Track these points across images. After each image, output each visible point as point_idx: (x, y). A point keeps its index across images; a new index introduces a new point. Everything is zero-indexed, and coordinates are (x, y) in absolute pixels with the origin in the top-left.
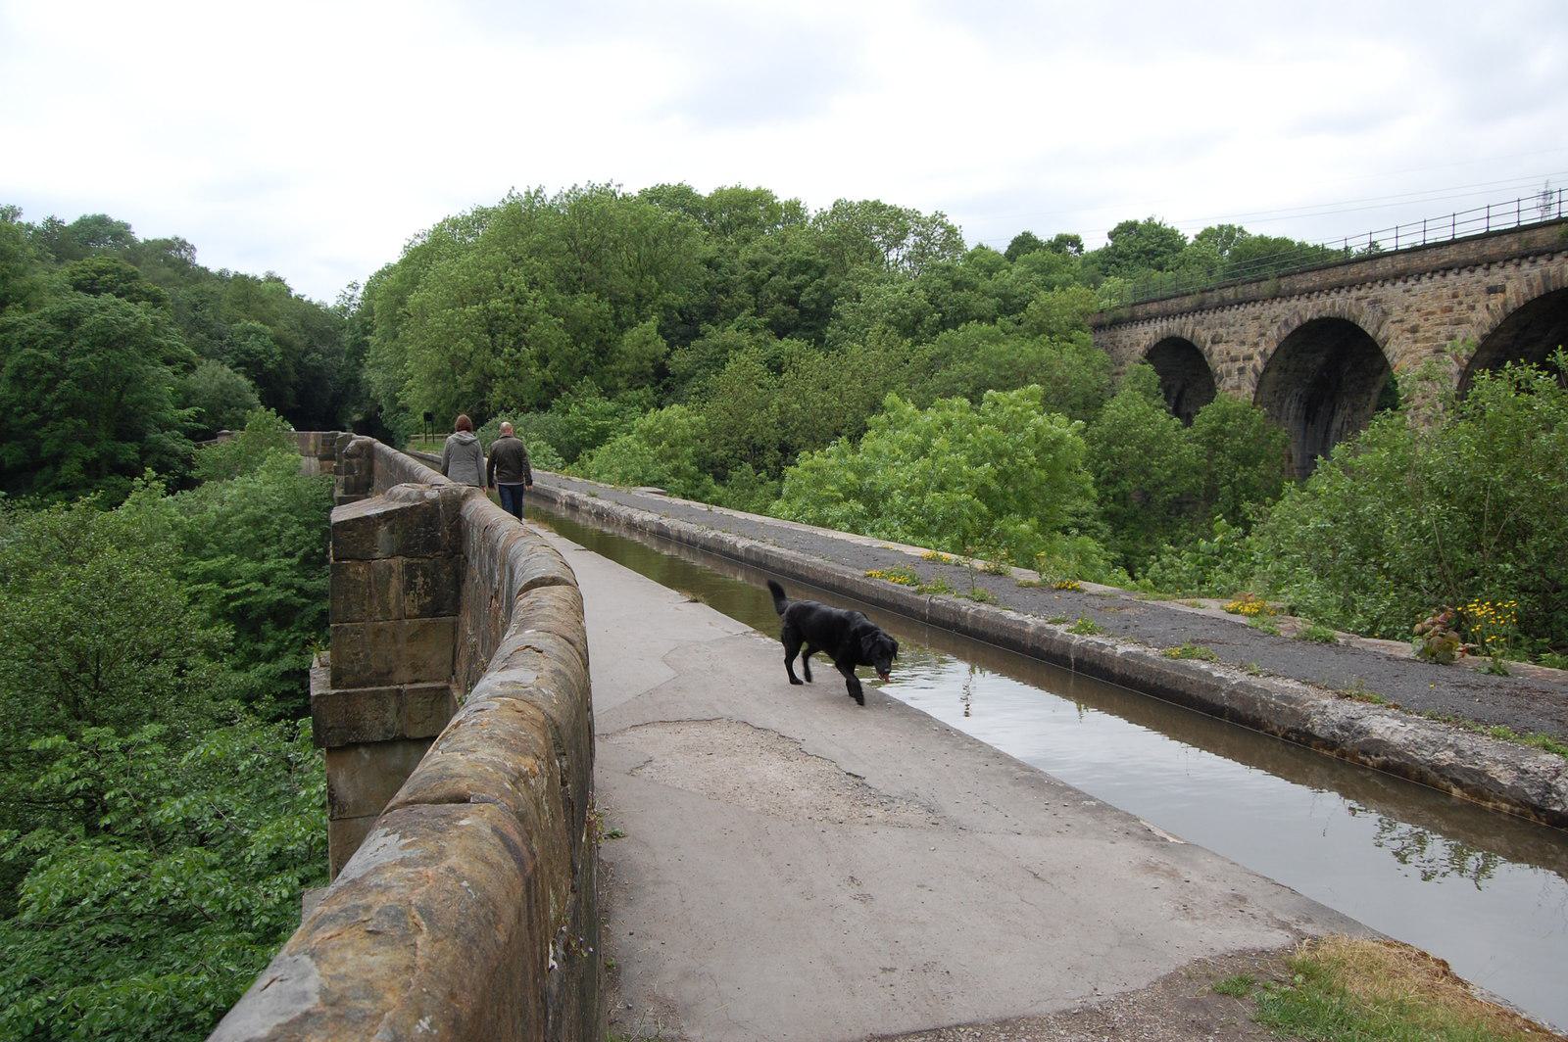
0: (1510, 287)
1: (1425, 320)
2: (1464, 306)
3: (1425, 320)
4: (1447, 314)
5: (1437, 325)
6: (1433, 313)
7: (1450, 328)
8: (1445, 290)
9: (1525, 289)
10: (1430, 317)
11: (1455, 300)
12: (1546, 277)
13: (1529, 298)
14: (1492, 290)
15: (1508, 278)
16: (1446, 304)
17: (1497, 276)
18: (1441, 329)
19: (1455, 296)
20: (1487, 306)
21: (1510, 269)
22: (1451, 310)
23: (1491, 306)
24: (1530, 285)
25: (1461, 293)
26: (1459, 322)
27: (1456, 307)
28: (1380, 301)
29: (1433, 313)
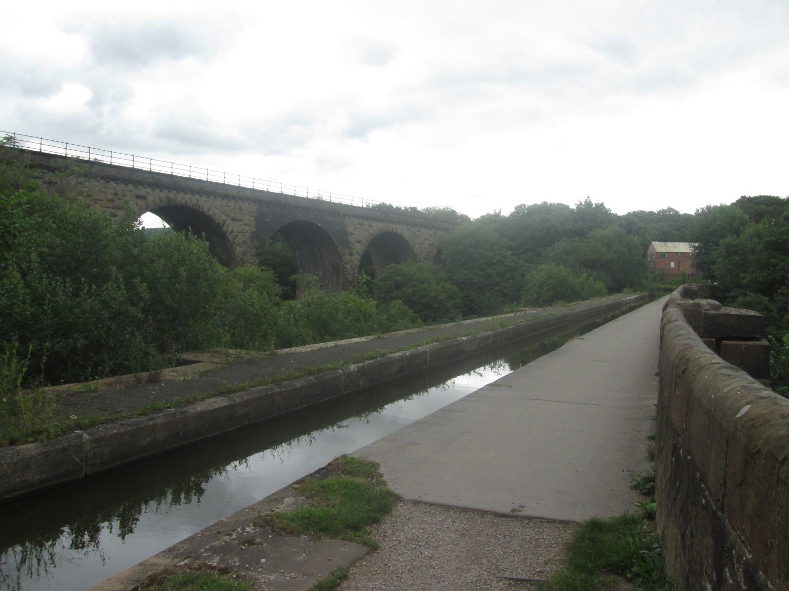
0: (150, 198)
1: (95, 203)
2: (122, 201)
3: (95, 203)
4: (111, 203)
5: (103, 207)
6: (100, 200)
7: (113, 210)
8: (108, 190)
9: (158, 201)
10: (99, 202)
11: (116, 197)
12: (168, 199)
13: (160, 205)
14: (138, 197)
15: (148, 194)
16: (110, 197)
17: (142, 191)
18: (107, 210)
19: (116, 194)
20: (137, 205)
21: (149, 190)
22: (113, 201)
23: (139, 205)
24: (160, 199)
25: (120, 194)
26: (119, 208)
27: (117, 200)
28: (55, 183)
29: (100, 200)
